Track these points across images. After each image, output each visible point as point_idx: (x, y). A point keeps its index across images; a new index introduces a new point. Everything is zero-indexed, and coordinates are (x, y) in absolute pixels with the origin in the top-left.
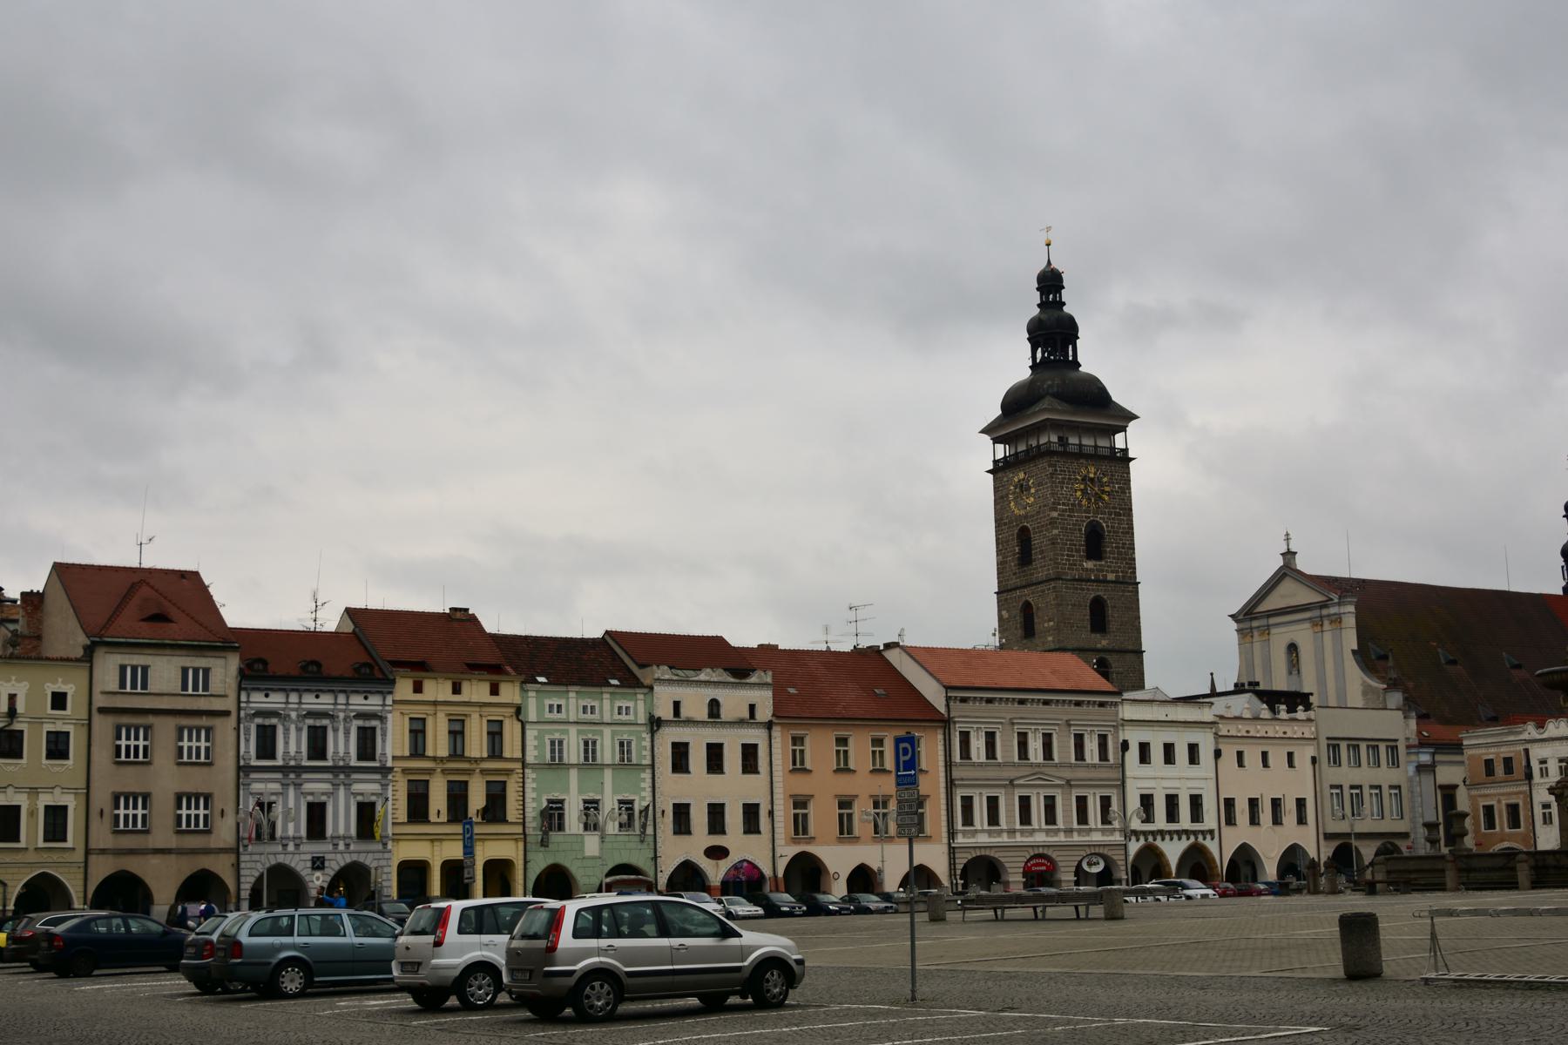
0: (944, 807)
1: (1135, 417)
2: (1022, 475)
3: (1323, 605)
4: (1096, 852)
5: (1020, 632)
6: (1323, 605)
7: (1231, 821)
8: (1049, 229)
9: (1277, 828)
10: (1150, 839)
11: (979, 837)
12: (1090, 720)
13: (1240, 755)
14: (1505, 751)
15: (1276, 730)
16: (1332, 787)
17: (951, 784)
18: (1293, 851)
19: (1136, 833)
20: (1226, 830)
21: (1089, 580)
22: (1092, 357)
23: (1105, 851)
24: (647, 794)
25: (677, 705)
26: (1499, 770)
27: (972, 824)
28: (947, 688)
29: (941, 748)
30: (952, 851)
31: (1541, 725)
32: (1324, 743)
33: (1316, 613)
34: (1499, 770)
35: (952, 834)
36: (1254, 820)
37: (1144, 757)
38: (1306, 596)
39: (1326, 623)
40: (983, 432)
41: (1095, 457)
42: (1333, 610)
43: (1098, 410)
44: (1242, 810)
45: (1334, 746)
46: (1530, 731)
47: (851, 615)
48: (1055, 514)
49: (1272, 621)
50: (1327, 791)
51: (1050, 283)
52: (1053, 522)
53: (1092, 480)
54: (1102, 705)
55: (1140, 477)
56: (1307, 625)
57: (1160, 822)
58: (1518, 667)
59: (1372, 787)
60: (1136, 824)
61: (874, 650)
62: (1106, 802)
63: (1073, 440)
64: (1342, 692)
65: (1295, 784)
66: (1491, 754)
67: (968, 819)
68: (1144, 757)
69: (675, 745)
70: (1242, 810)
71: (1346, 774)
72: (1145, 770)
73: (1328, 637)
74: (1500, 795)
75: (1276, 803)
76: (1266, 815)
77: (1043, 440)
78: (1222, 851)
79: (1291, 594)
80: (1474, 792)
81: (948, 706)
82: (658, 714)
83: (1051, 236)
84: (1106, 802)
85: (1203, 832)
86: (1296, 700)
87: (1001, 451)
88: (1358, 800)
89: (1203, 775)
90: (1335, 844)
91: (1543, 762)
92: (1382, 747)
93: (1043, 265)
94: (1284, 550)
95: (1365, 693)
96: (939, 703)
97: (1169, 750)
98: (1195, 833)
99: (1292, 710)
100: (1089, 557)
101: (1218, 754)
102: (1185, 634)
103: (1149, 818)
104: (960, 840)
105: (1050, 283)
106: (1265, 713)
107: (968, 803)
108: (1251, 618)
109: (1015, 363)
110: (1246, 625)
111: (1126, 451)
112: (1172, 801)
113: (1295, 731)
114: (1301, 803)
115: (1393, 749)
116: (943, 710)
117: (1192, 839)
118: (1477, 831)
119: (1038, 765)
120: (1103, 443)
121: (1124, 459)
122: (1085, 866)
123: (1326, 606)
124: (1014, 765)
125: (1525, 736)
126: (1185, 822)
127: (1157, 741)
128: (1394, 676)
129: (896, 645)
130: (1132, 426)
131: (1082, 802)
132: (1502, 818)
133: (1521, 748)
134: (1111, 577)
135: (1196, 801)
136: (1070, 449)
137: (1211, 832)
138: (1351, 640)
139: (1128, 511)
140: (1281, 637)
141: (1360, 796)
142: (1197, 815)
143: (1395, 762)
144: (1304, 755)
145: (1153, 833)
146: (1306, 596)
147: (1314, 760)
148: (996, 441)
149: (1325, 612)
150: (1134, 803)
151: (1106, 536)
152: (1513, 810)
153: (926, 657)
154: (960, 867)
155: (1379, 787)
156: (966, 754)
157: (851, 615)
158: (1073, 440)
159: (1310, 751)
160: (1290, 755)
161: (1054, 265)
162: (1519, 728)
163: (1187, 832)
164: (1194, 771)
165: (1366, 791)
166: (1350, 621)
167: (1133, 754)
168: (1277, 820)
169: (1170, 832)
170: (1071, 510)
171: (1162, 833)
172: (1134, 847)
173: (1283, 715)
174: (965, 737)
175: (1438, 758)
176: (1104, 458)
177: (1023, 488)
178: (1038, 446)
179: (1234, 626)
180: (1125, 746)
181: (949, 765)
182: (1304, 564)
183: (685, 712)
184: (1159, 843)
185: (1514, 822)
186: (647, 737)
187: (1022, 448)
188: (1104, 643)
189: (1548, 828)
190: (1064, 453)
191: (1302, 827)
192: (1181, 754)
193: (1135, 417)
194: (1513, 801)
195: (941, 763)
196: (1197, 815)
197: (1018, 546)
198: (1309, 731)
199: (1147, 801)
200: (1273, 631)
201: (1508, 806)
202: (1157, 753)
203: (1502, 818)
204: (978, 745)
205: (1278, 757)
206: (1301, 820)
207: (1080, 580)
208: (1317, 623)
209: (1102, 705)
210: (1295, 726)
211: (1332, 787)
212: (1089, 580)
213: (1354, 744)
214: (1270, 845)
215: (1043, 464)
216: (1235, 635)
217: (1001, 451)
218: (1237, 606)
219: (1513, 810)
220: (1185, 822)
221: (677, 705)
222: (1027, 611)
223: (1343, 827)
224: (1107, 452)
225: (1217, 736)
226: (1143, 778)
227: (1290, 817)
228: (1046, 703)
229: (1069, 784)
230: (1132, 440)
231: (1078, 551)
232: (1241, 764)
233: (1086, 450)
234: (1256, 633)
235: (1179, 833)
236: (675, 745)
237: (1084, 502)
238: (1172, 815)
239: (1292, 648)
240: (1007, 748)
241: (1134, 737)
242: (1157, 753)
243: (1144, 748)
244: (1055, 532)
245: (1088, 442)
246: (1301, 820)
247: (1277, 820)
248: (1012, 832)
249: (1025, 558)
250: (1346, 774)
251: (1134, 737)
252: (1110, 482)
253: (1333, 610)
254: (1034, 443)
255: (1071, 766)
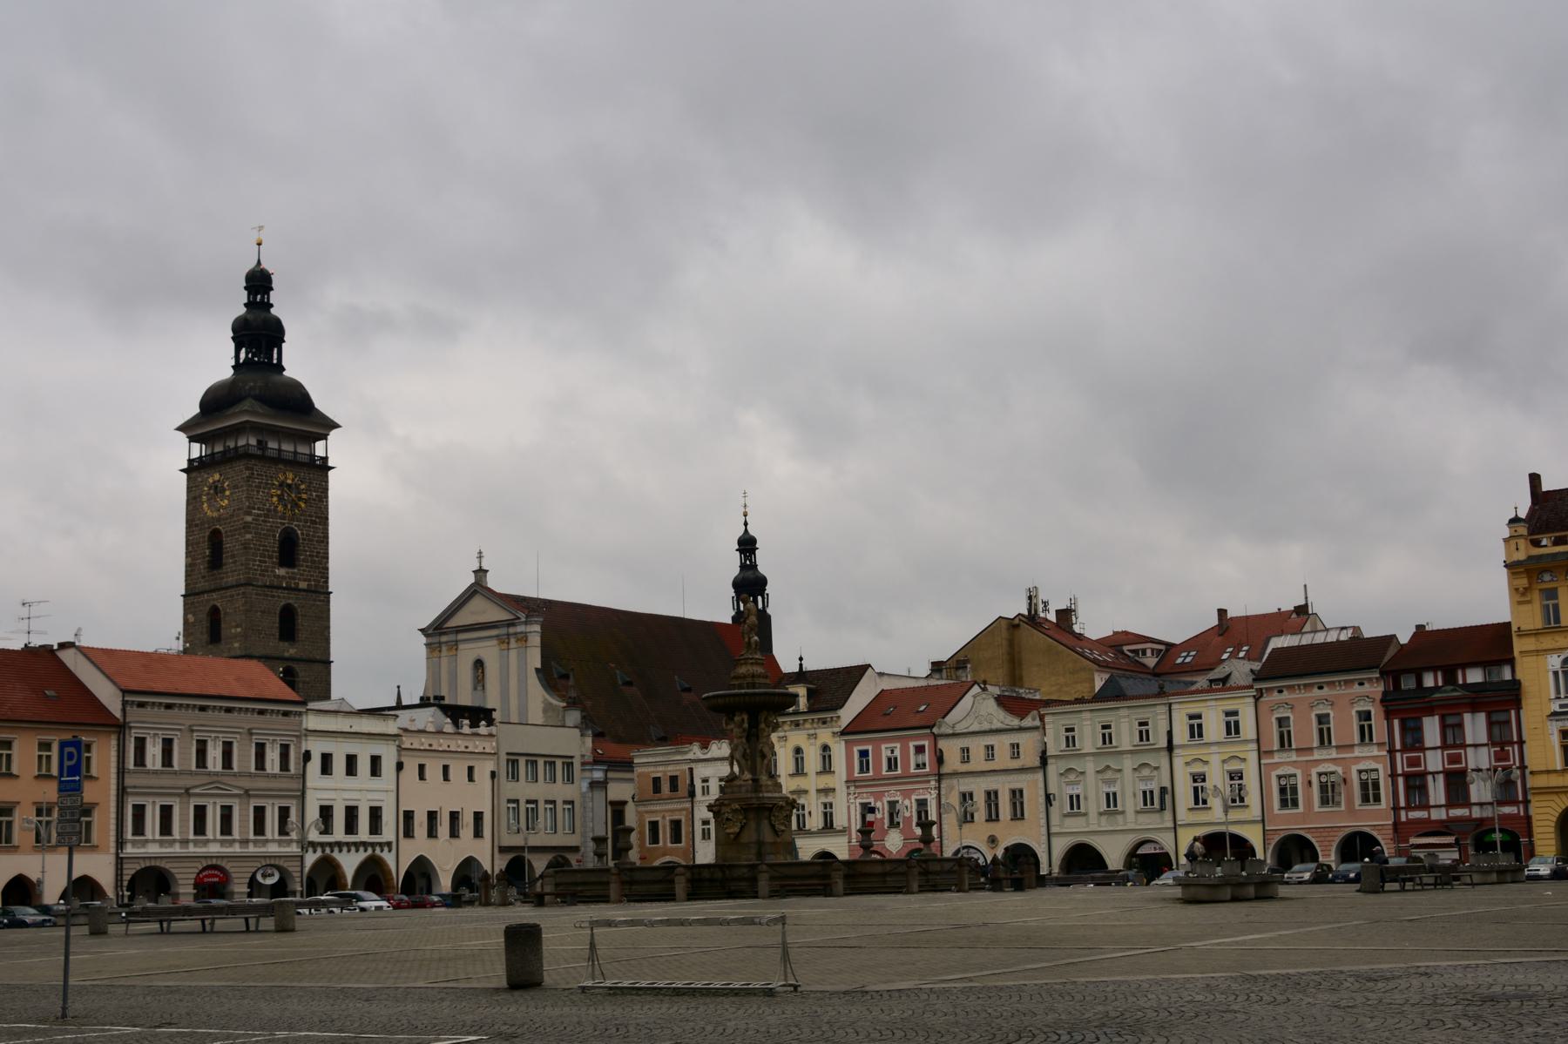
0: (113, 815)
1: (336, 426)
2: (217, 477)
3: (510, 624)
4: (271, 863)
5: (205, 637)
6: (510, 624)
7: (409, 833)
8: (261, 228)
9: (454, 841)
10: (328, 850)
11: (150, 847)
12: (273, 729)
13: (422, 767)
14: (672, 770)
15: (459, 744)
16: (509, 801)
17: (122, 792)
18: (469, 863)
19: (313, 845)
20: (404, 842)
21: (280, 588)
22: (297, 361)
23: (281, 863)
26: (666, 787)
27: (143, 834)
28: (125, 692)
29: (114, 753)
30: (120, 862)
31: (705, 746)
32: (504, 757)
33: (503, 631)
34: (666, 787)
35: (120, 843)
36: (432, 833)
37: (326, 767)
38: (496, 614)
39: (513, 641)
40: (179, 429)
42: (520, 629)
43: (300, 415)
44: (420, 822)
45: (513, 762)
46: (695, 751)
47: (24, 612)
48: (249, 519)
49: (461, 636)
50: (504, 805)
51: (259, 283)
52: (246, 526)
53: (289, 486)
54: (286, 714)
55: (338, 485)
56: (495, 642)
57: (339, 834)
58: (688, 690)
59: (547, 802)
60: (314, 836)
61: (47, 650)
62: (284, 813)
63: (273, 445)
64: (523, 709)
65: (474, 797)
66: (659, 772)
67: (139, 829)
68: (326, 767)
70: (420, 822)
71: (523, 789)
72: (326, 782)
73: (513, 654)
74: (664, 812)
75: (454, 816)
76: (444, 828)
77: (241, 442)
78: (398, 863)
79: (481, 611)
80: (642, 809)
81: (124, 710)
83: (263, 236)
84: (284, 813)
85: (381, 844)
86: (479, 715)
87: (197, 450)
88: (533, 814)
89: (385, 787)
90: (509, 857)
91: (705, 780)
92: (559, 763)
93: (251, 265)
94: (476, 567)
95: (545, 711)
96: (115, 708)
97: (351, 762)
98: (373, 845)
99: (474, 725)
100: (282, 564)
101: (400, 766)
102: (374, 647)
103: (327, 829)
104: (129, 850)
105: (259, 283)
106: (449, 728)
107: (139, 811)
108: (440, 632)
109: (217, 361)
110: (435, 640)
111: (325, 459)
112: (351, 813)
113: (478, 745)
114: (478, 816)
115: (569, 766)
116: (118, 714)
117: (370, 851)
118: (642, 845)
119: (216, 774)
120: (303, 449)
121: (323, 467)
122: (259, 878)
123: (513, 625)
124: (191, 773)
125: (690, 756)
126: (363, 834)
127: (339, 752)
128: (573, 694)
129: (70, 645)
130: (333, 434)
131: (260, 813)
132: (665, 833)
133: (686, 767)
134: (303, 585)
135: (375, 813)
136: (269, 453)
137: (389, 844)
138: (535, 659)
139: (324, 520)
140: (468, 653)
141: (535, 811)
142: (375, 827)
143: (570, 779)
144: (484, 769)
145: (331, 845)
146: (496, 614)
147: (493, 775)
148: (192, 439)
149: (512, 630)
150: (313, 814)
151: (300, 543)
152: (676, 825)
153: (102, 658)
154: (127, 878)
155: (553, 802)
156: (140, 759)
157: (24, 612)
158: (273, 445)
159: (490, 766)
160: (471, 769)
161: (265, 265)
162: (686, 748)
163: (365, 844)
164: (376, 783)
165: (541, 805)
166: (535, 640)
167: (315, 765)
168: (454, 834)
169: (348, 844)
170: (266, 516)
171: (340, 845)
172: (311, 858)
173: (466, 730)
174: (141, 744)
175: (610, 775)
176: (302, 465)
177: (217, 489)
178: (236, 448)
179: (423, 640)
180: (307, 756)
181: (122, 771)
182: (493, 582)
184: (336, 854)
185: (676, 838)
187: (219, 448)
188: (292, 652)
189: (706, 843)
190: (262, 456)
191: (478, 841)
192: (364, 766)
193: (336, 426)
194: (676, 817)
195: (113, 770)
196: (375, 827)
197: (208, 549)
198: (489, 746)
199: (326, 812)
200: (461, 646)
201: (672, 822)
202: (339, 765)
203: (665, 833)
204: (154, 752)
205: (458, 771)
206: (478, 833)
207: (271, 587)
208: (504, 640)
209: (286, 714)
210: (478, 741)
211: (509, 801)
212: (280, 588)
213: (532, 759)
214: (445, 858)
215: (240, 466)
216: (424, 649)
217: (197, 450)
218: (427, 620)
219: (676, 825)
220: (363, 834)
222: (215, 615)
223: (517, 841)
224: (306, 459)
225: (400, 749)
226: (322, 789)
228: (229, 710)
229: (247, 794)
230: (332, 448)
231: (270, 557)
232: (422, 777)
233: (286, 456)
234: (444, 648)
235: (357, 845)
237: (280, 508)
238: (351, 827)
239: (479, 664)
240: (184, 756)
241: (317, 747)
242: (339, 765)
243: (326, 760)
244: (248, 536)
245: (287, 447)
246: (478, 833)
247: (454, 834)
248: (184, 842)
249: (216, 562)
250: (523, 789)
251: (317, 747)
252: (308, 490)
253: (520, 629)
254: (231, 444)
255: (250, 775)
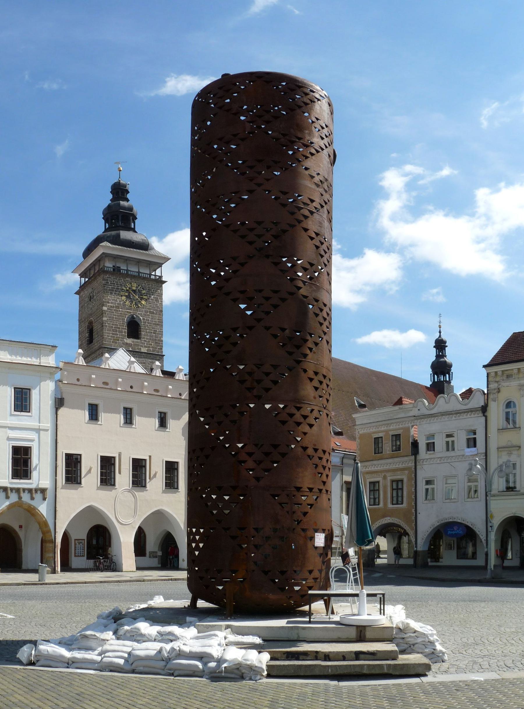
41: (138, 277)
44: (90, 467)
53: (134, 291)
70: (90, 467)
75: (139, 466)
76: (124, 476)
85: (30, 491)
100: (129, 336)
114: (171, 468)
137: (43, 491)
176: (144, 278)
227: (156, 481)
237: (128, 303)
249: (91, 340)
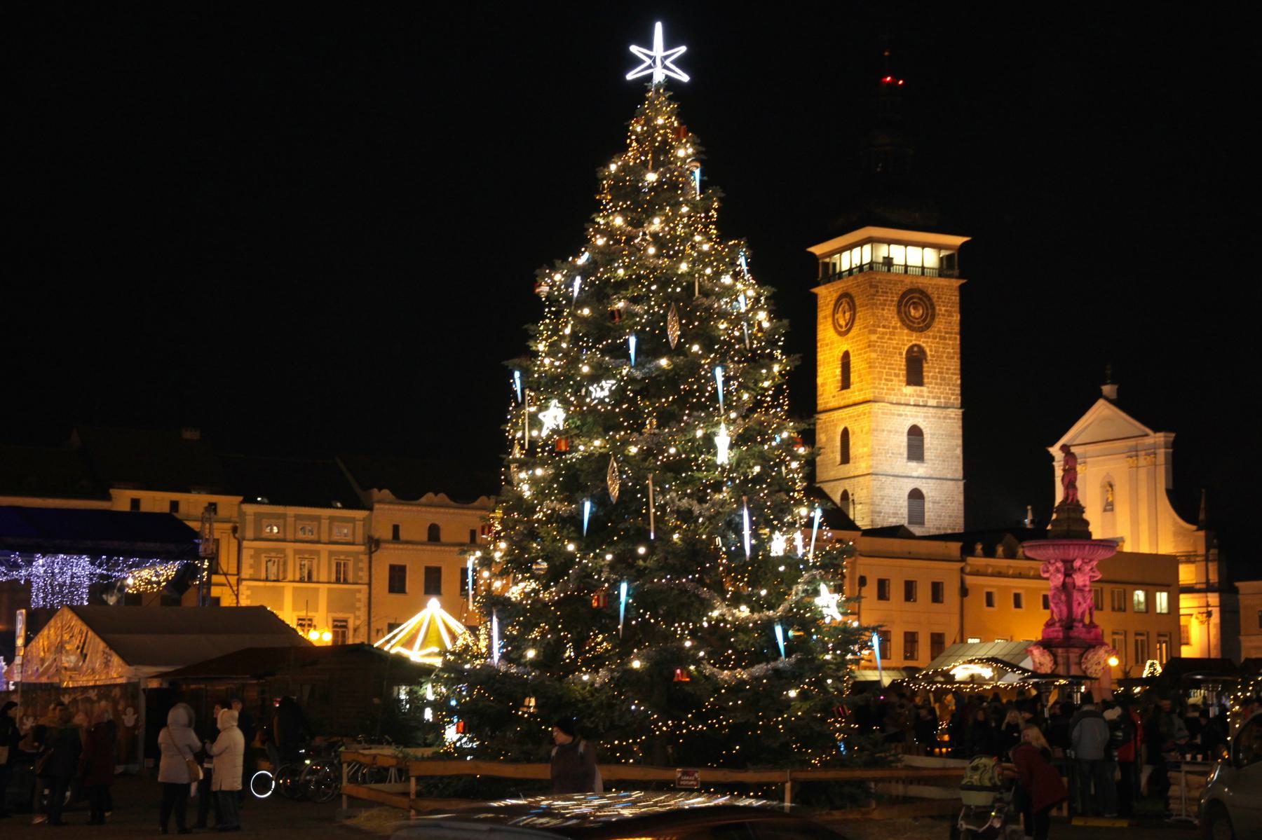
24: (363, 614)
25: (396, 529)
69: (393, 568)
82: (376, 536)
101: (964, 591)
183: (403, 535)
186: (365, 558)
221: (396, 529)
231: (897, 375)
236: (393, 568)
242: (897, 591)
